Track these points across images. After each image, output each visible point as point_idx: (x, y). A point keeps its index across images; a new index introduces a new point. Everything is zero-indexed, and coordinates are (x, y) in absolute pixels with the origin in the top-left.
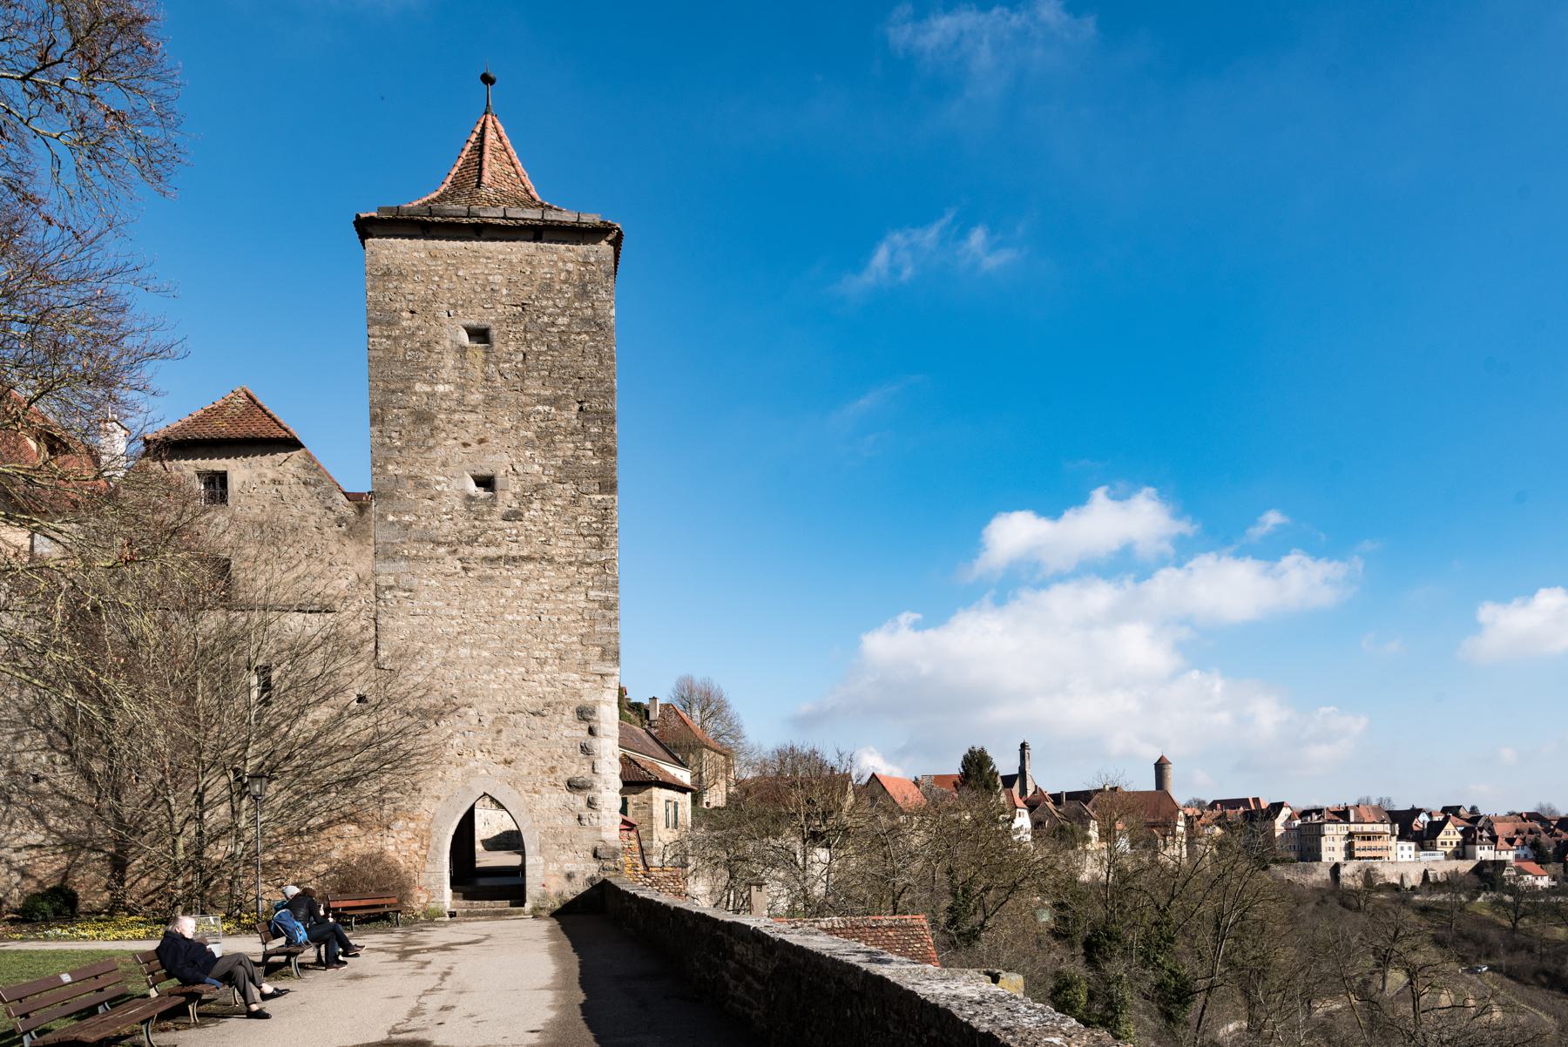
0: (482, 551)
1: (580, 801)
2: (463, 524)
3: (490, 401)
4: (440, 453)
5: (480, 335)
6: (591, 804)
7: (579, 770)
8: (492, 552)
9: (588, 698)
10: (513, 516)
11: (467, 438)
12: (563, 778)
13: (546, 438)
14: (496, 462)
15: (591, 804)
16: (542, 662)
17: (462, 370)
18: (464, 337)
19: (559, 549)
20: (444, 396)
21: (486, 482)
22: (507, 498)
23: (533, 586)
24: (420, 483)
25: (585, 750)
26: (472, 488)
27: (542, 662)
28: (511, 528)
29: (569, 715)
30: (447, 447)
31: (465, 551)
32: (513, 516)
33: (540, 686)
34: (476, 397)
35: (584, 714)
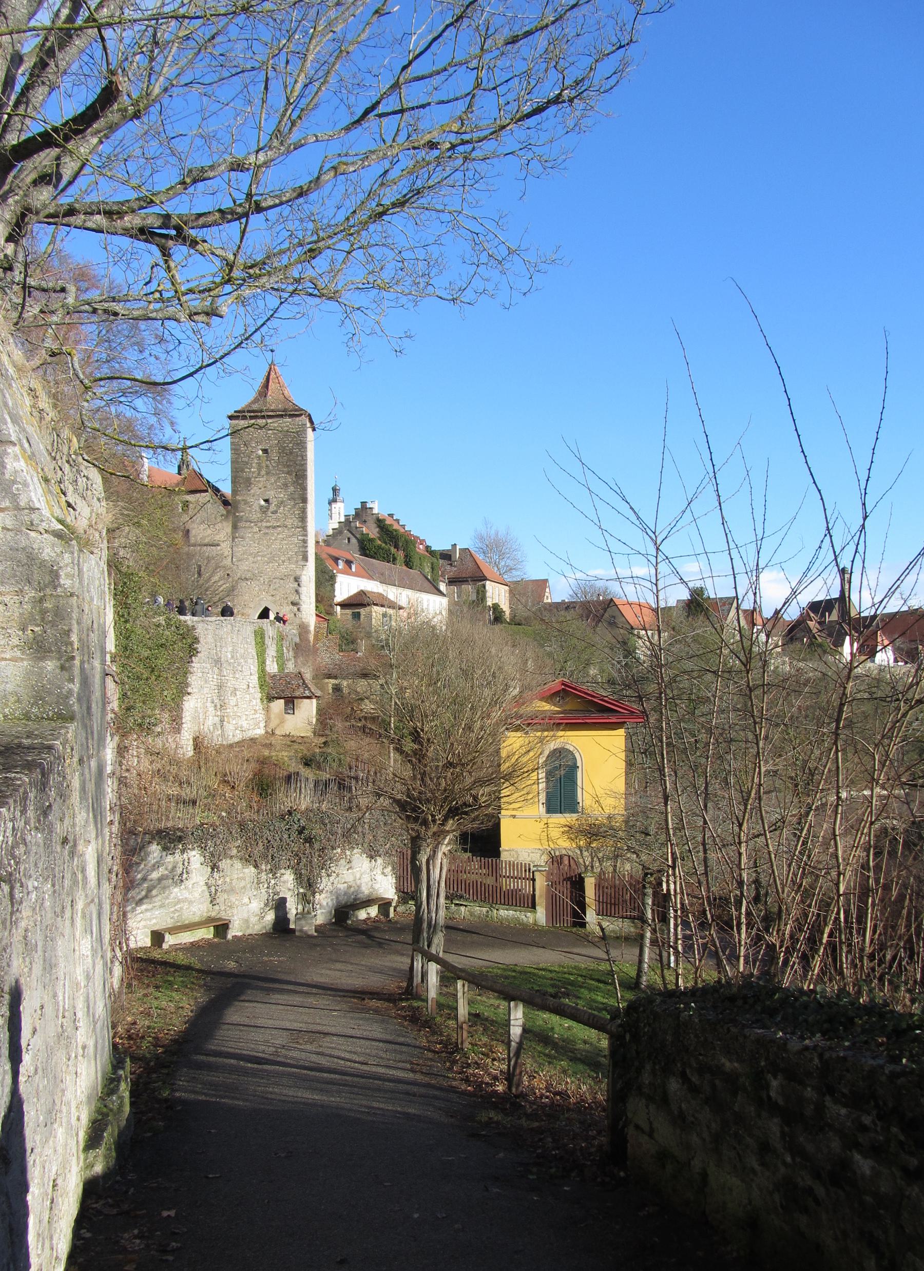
0: (265, 524)
1: (295, 608)
2: (259, 515)
3: (267, 474)
4: (252, 491)
5: (265, 451)
6: (298, 609)
7: (294, 598)
8: (268, 524)
9: (298, 573)
10: (275, 512)
11: (260, 486)
12: (290, 600)
13: (285, 485)
14: (270, 494)
15: (298, 609)
16: (283, 562)
17: (259, 464)
18: (260, 452)
19: (289, 522)
20: (253, 473)
21: (266, 501)
22: (273, 507)
23: (281, 536)
24: (246, 502)
25: (297, 591)
26: (263, 503)
27: (283, 562)
28: (274, 516)
29: (292, 579)
30: (254, 490)
31: (260, 524)
32: (275, 512)
33: (283, 570)
34: (263, 472)
35: (297, 579)
